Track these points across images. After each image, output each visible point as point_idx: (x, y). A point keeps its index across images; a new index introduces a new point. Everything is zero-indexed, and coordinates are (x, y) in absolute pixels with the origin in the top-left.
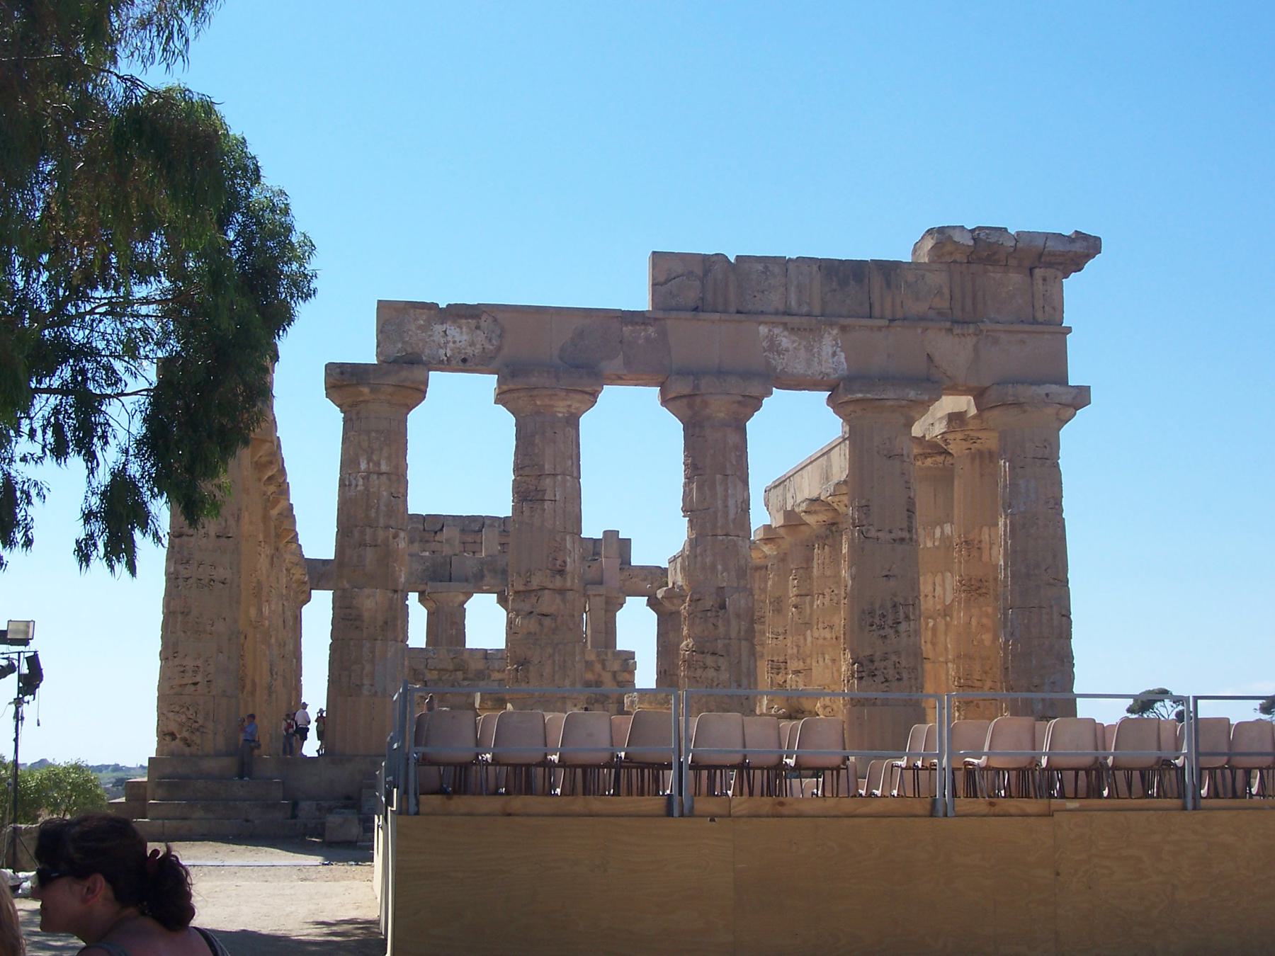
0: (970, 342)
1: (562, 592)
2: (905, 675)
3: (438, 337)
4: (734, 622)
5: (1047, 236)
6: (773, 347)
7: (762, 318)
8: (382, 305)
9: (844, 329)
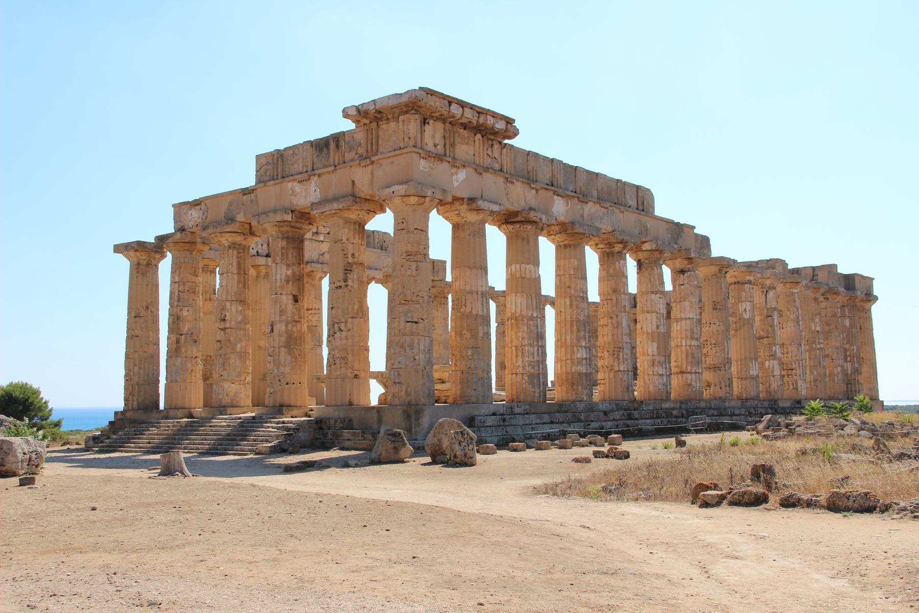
0: (370, 167)
1: (224, 329)
2: (338, 362)
3: (190, 217)
4: (276, 338)
5: (389, 97)
6: (294, 193)
7: (290, 178)
8: (174, 206)
9: (319, 175)
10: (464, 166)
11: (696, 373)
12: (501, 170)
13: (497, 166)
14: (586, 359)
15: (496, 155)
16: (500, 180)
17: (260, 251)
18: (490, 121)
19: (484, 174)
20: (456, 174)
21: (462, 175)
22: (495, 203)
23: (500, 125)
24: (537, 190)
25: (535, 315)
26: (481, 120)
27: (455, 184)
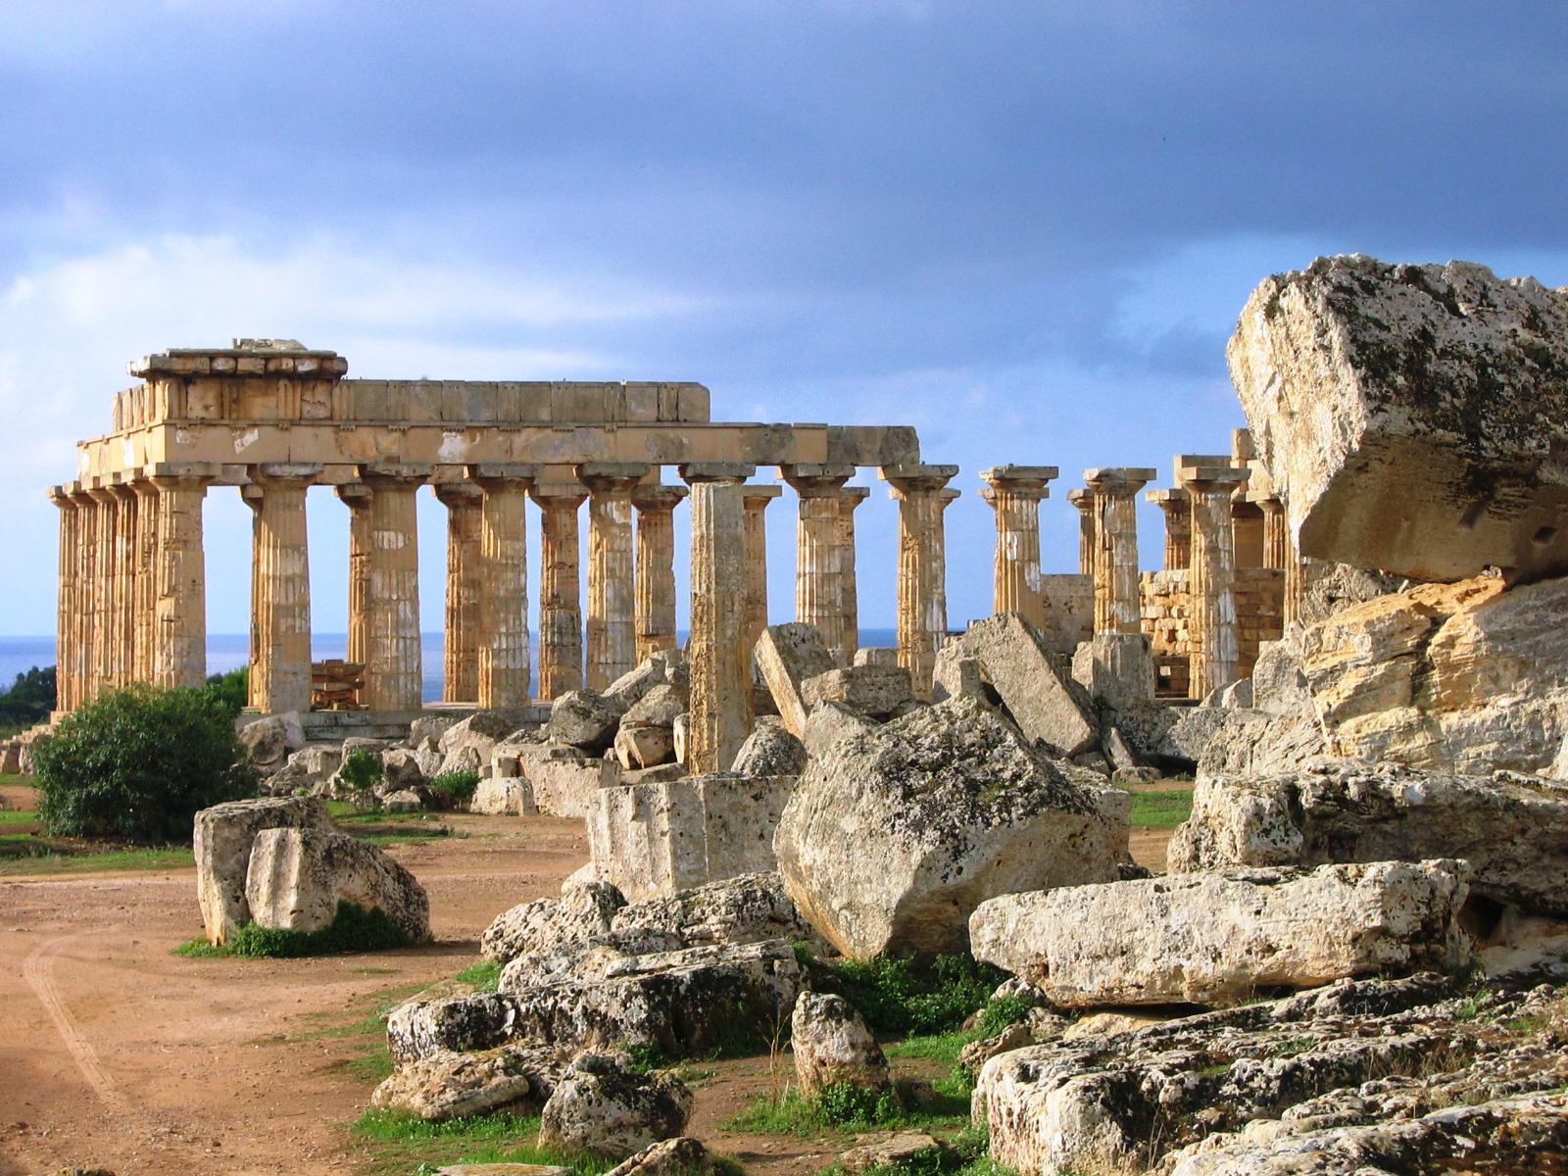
10: (255, 425)
12: (331, 418)
14: (507, 650)
15: (322, 398)
16: (327, 433)
18: (287, 364)
19: (296, 430)
20: (241, 437)
21: (251, 437)
22: (305, 464)
23: (306, 367)
24: (404, 432)
25: (395, 597)
26: (272, 366)
27: (238, 449)
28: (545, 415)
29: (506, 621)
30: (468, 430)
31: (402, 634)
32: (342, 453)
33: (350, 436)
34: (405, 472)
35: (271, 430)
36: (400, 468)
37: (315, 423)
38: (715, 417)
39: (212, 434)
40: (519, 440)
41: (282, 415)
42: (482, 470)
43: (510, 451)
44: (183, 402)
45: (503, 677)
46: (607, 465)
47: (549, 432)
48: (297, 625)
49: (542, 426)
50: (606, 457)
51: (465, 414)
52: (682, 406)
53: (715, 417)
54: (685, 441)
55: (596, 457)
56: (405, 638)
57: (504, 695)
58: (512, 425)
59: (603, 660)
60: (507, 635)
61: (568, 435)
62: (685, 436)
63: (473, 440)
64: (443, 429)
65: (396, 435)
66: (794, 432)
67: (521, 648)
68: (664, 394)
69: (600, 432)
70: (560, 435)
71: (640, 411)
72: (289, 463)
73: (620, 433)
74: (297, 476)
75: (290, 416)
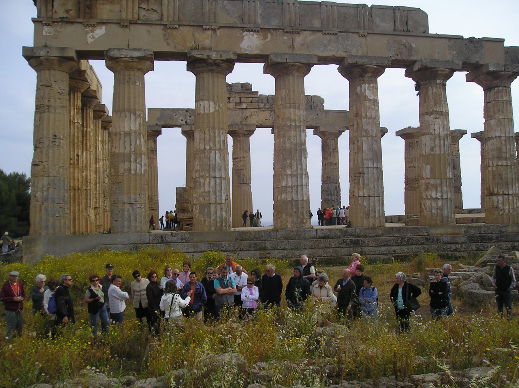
10: (103, 23)
11: (504, 194)
13: (154, 17)
14: (292, 187)
16: (158, 31)
17: (188, 121)
19: (132, 27)
20: (92, 31)
21: (100, 31)
22: (139, 50)
24: (214, 30)
27: (90, 40)
28: (317, 24)
29: (291, 166)
30: (263, 31)
31: (212, 174)
32: (168, 44)
33: (175, 32)
34: (214, 56)
35: (115, 28)
36: (210, 53)
37: (147, 23)
38: (433, 30)
39: (70, 28)
40: (299, 39)
41: (124, 16)
42: (272, 57)
43: (292, 47)
44: (50, 7)
45: (289, 206)
46: (362, 57)
47: (319, 34)
48: (133, 167)
49: (314, 31)
50: (360, 53)
51: (259, 21)
52: (410, 23)
53: (433, 30)
54: (414, 45)
55: (354, 53)
56: (215, 177)
57: (290, 219)
58: (293, 30)
59: (361, 194)
60: (291, 175)
61: (335, 37)
62: (414, 43)
63: (265, 38)
64: (243, 29)
65: (210, 32)
66: (484, 44)
67: (302, 185)
68: (398, 14)
69: (355, 36)
70: (328, 37)
71: (382, 24)
72: (128, 49)
73: (369, 37)
74: (132, 58)
75: (130, 18)
